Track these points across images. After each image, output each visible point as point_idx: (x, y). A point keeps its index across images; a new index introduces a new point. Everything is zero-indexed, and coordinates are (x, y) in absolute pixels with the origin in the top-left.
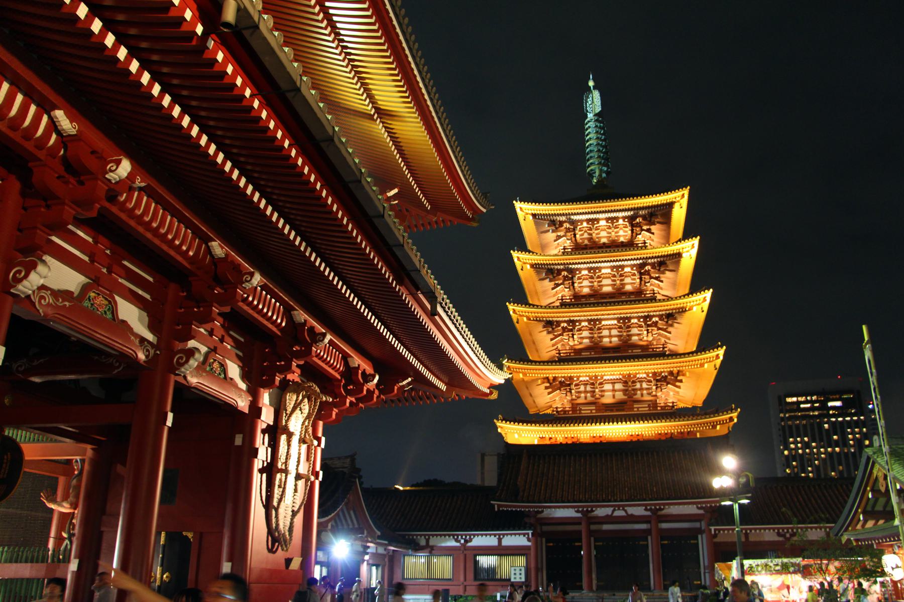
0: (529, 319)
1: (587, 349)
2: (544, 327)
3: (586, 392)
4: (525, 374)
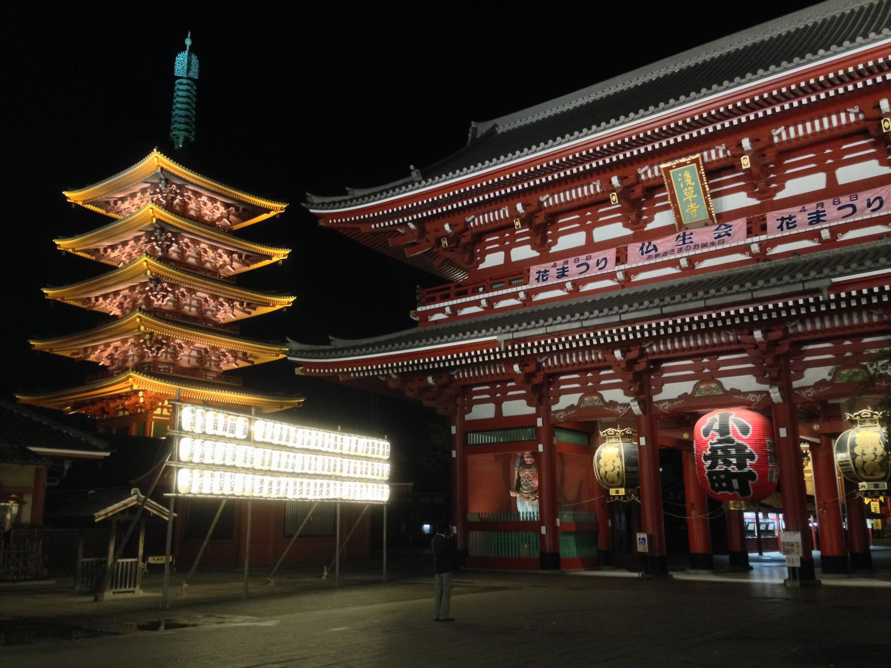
1: (170, 312)
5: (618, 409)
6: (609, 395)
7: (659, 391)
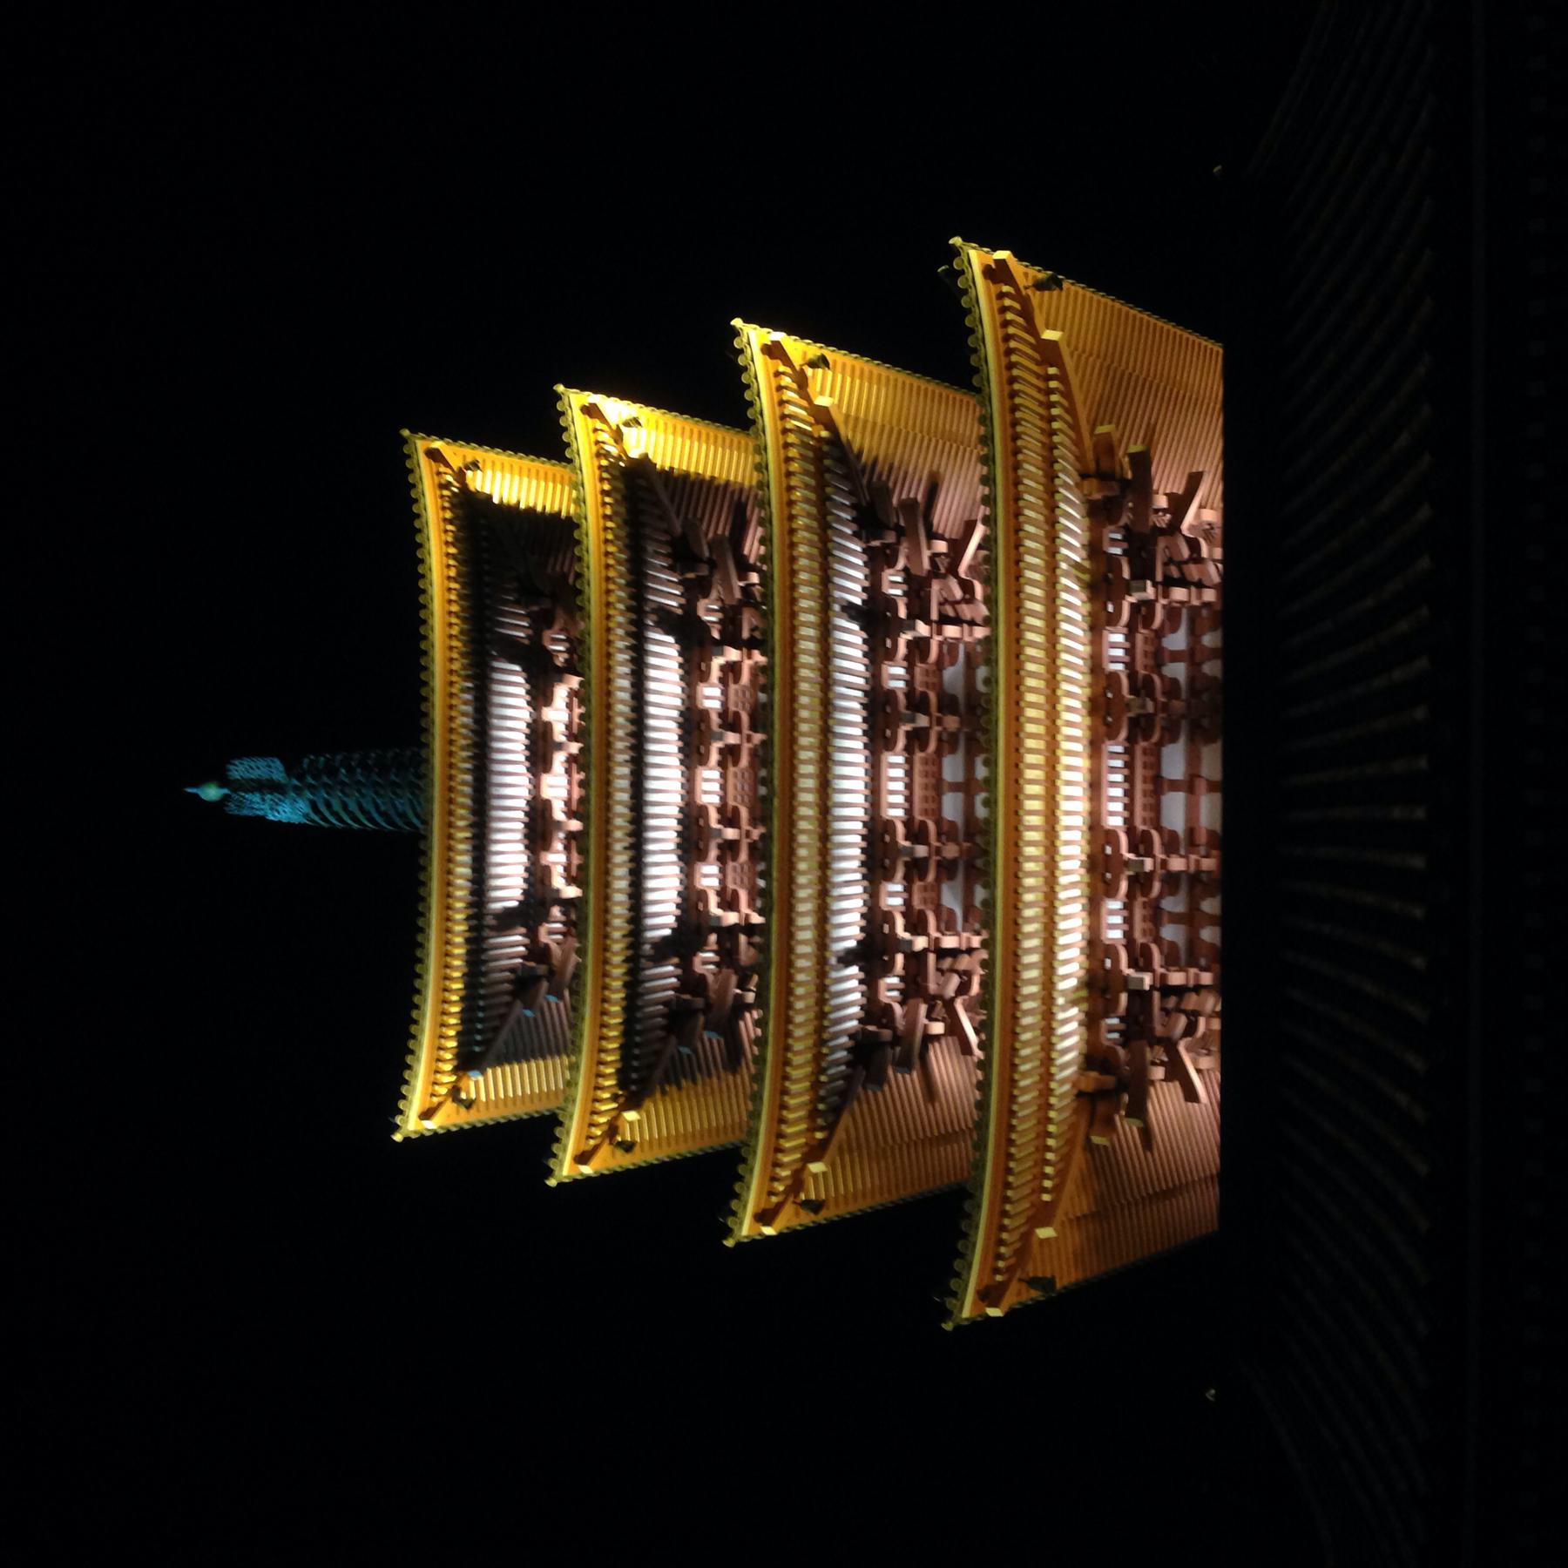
0: (815, 1152)
2: (879, 1080)
3: (1191, 919)
4: (1043, 1215)
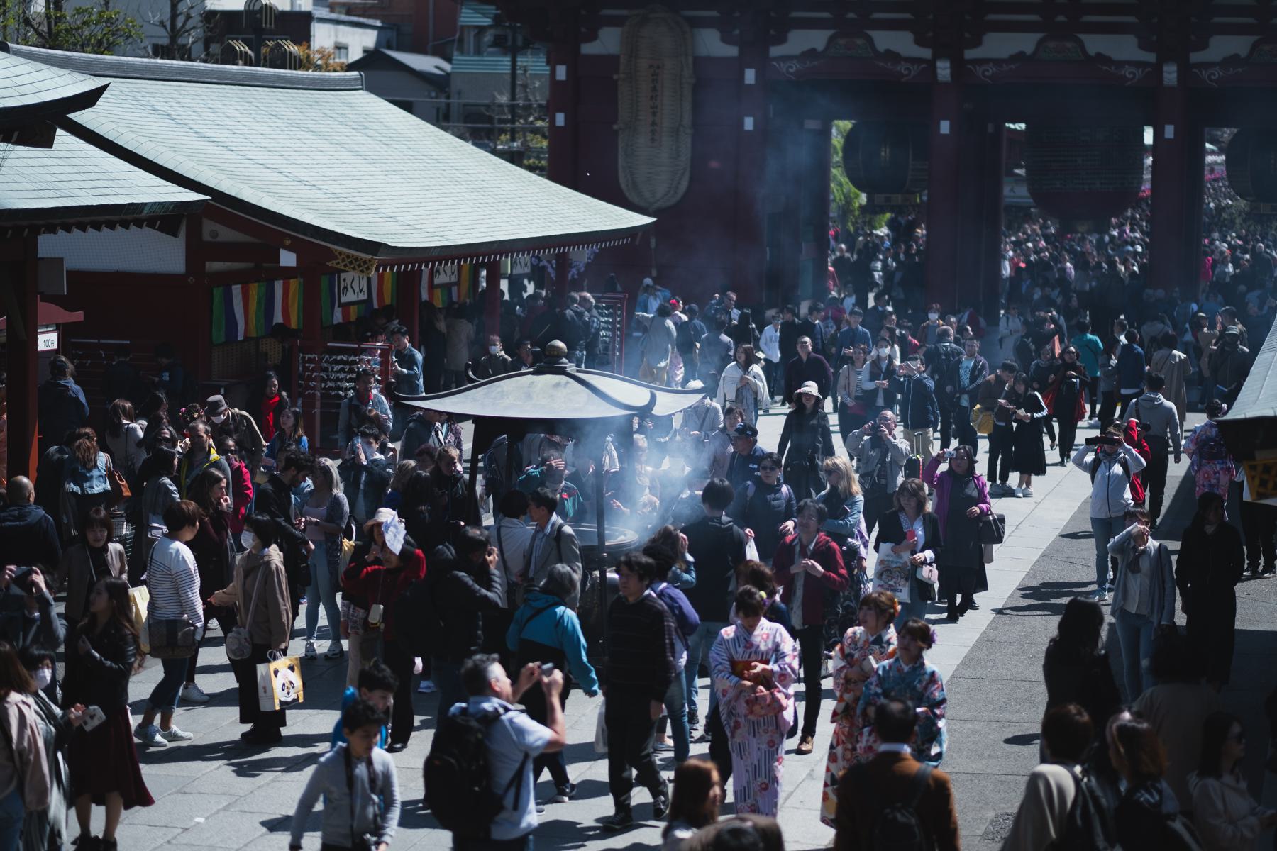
5: (902, 68)
6: (884, 40)
7: (977, 43)
